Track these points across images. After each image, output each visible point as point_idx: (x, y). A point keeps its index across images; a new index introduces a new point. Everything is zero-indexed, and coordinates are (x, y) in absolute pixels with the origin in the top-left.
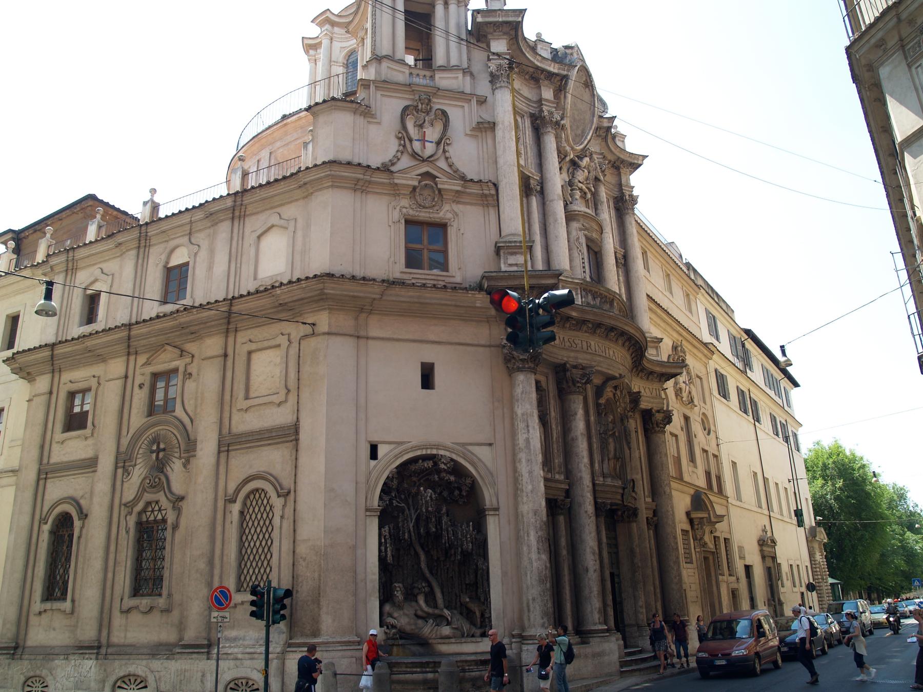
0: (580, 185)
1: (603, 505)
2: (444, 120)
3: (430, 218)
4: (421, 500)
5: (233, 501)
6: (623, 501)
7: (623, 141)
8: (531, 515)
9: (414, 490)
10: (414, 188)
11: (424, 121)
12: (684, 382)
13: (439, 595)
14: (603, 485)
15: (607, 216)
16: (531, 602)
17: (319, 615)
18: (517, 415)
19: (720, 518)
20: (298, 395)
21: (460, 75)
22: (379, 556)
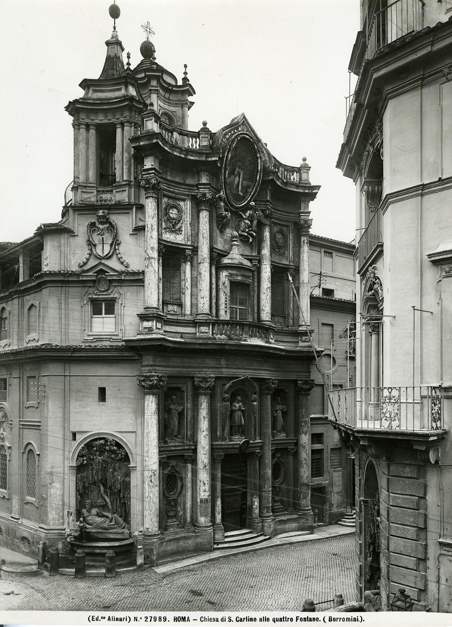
22: (76, 488)
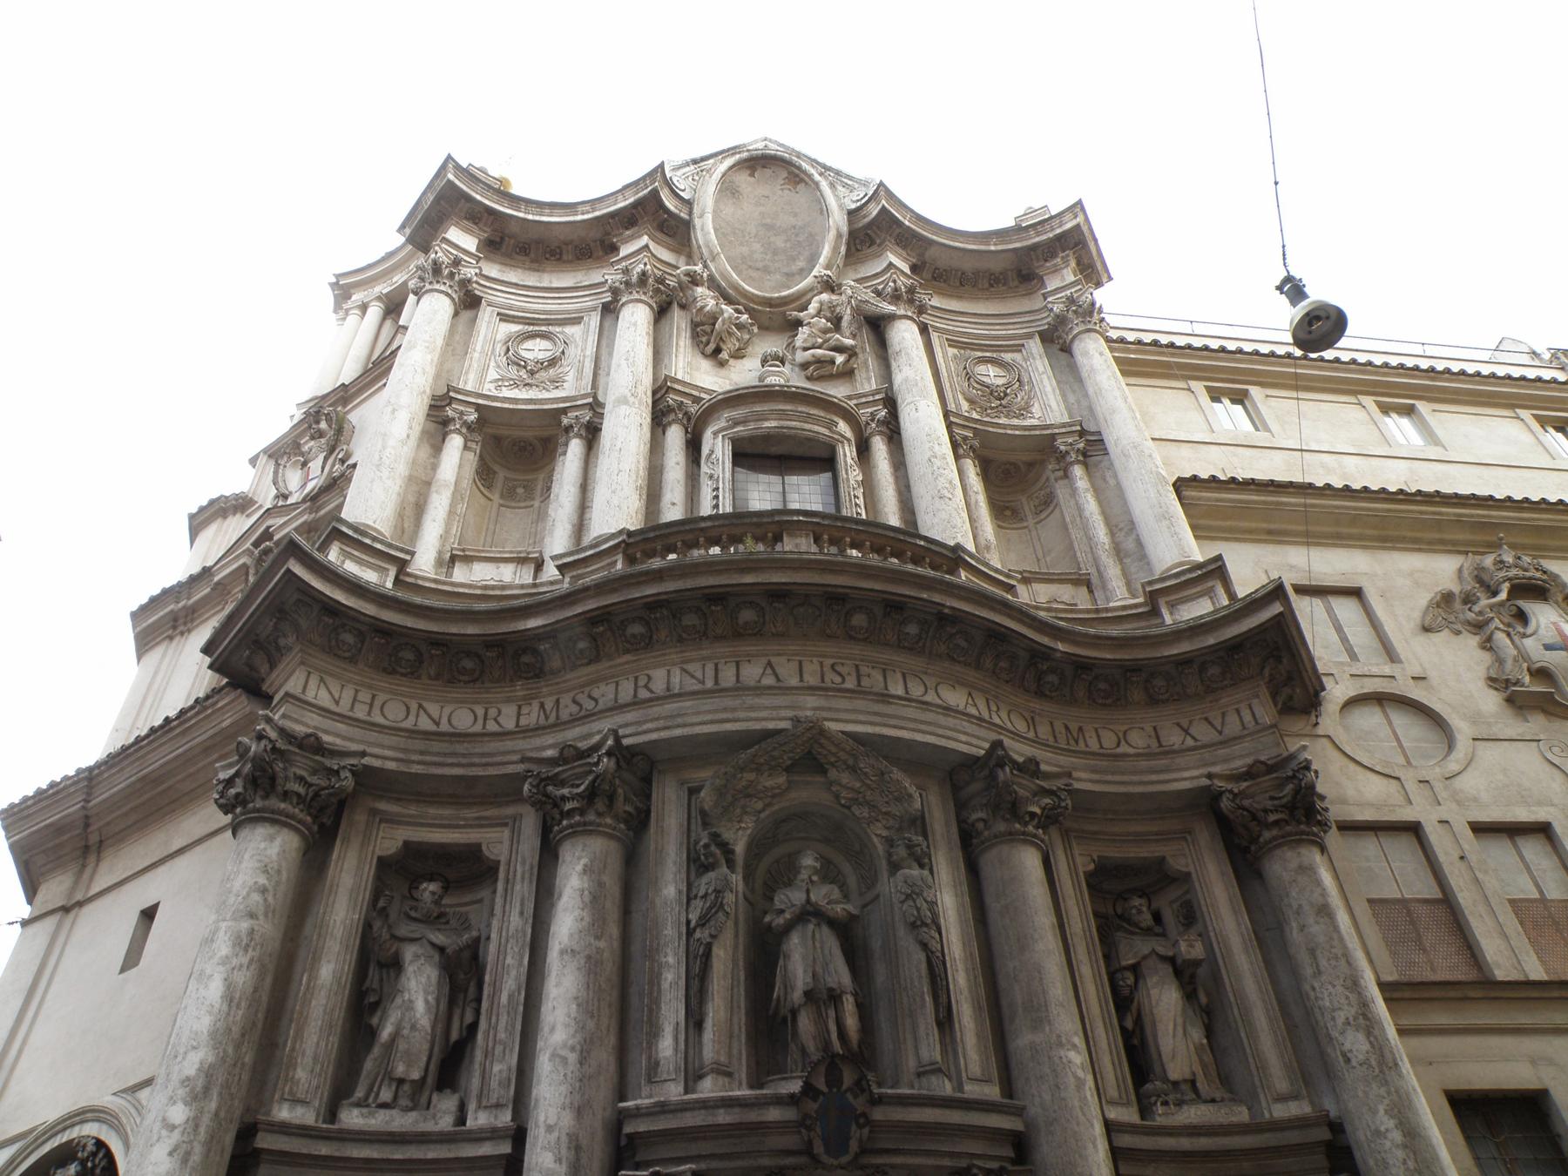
6: (808, 1151)
12: (1548, 647)
14: (663, 1109)
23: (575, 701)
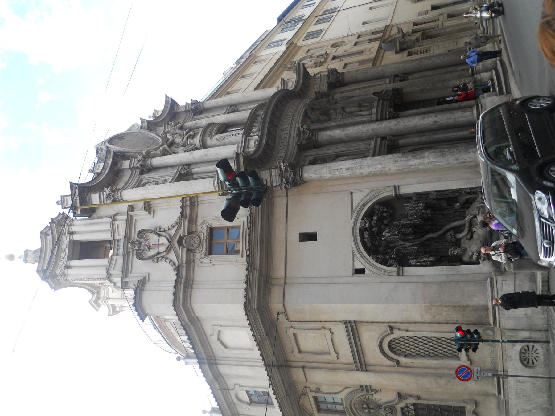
0: (185, 139)
1: (391, 113)
2: (144, 232)
3: (207, 239)
4: (390, 239)
5: (398, 363)
6: (387, 100)
7: (158, 111)
8: (398, 164)
9: (384, 243)
10: (189, 250)
11: (146, 245)
13: (456, 224)
15: (203, 121)
16: (458, 161)
17: (473, 306)
18: (331, 177)
19: (400, 30)
20: (325, 322)
21: (116, 222)
23: (283, 143)
